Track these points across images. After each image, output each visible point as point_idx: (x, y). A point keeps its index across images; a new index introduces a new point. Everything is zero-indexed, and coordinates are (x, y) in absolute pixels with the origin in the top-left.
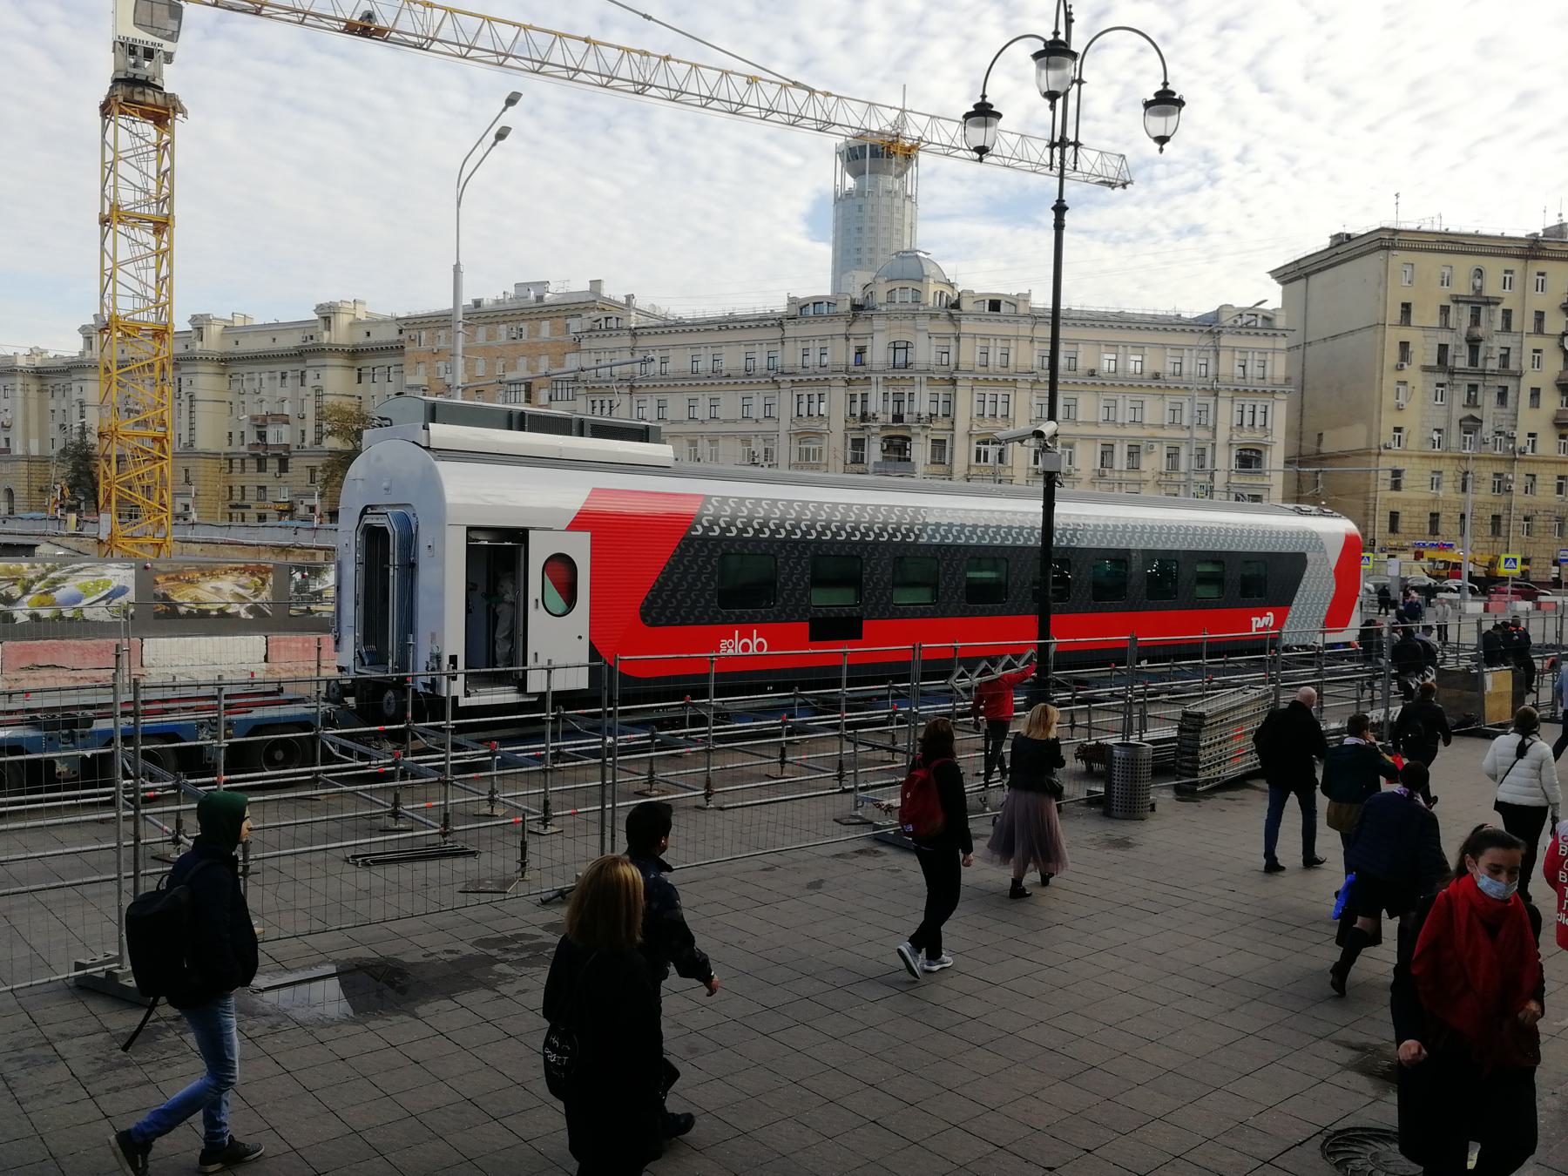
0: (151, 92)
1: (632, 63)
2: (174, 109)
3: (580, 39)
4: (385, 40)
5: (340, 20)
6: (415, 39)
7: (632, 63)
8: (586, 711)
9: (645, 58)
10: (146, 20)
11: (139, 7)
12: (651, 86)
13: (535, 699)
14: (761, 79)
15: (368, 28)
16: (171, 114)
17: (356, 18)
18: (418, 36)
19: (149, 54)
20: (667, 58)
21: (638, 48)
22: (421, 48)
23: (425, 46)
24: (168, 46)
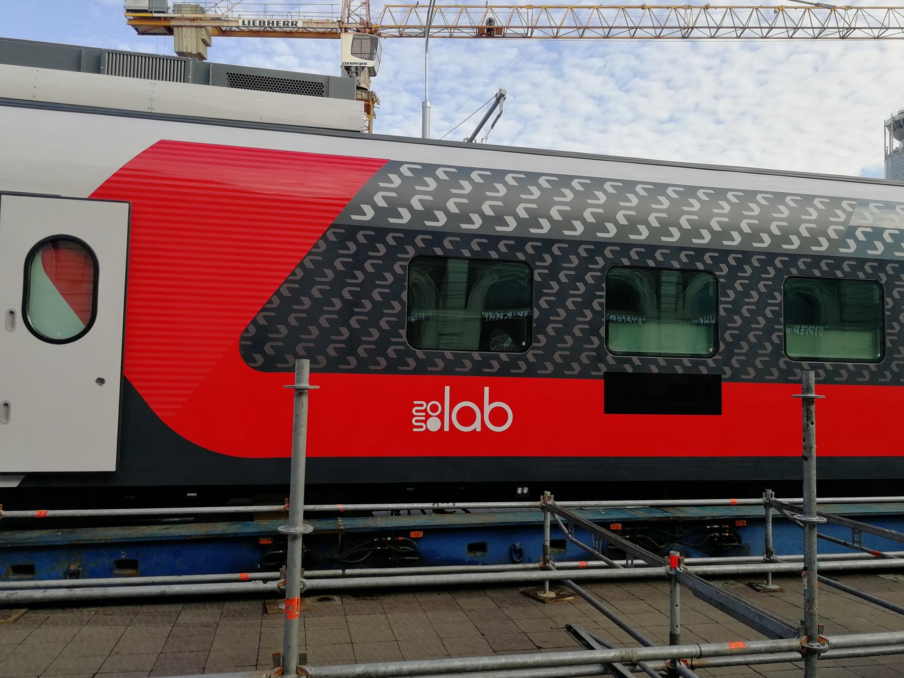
0: (360, 92)
1: (679, 16)
2: (372, 100)
3: (638, 7)
4: (503, 37)
5: (473, 27)
6: (521, 31)
7: (679, 16)
8: (51, 513)
9: (689, 11)
10: (358, 50)
11: (355, 44)
12: (693, 28)
13: (14, 484)
14: (786, 7)
15: (489, 30)
16: (371, 104)
17: (484, 24)
18: (524, 28)
19: (359, 70)
20: (707, 7)
21: (682, 4)
22: (525, 36)
23: (529, 35)
24: (370, 64)
